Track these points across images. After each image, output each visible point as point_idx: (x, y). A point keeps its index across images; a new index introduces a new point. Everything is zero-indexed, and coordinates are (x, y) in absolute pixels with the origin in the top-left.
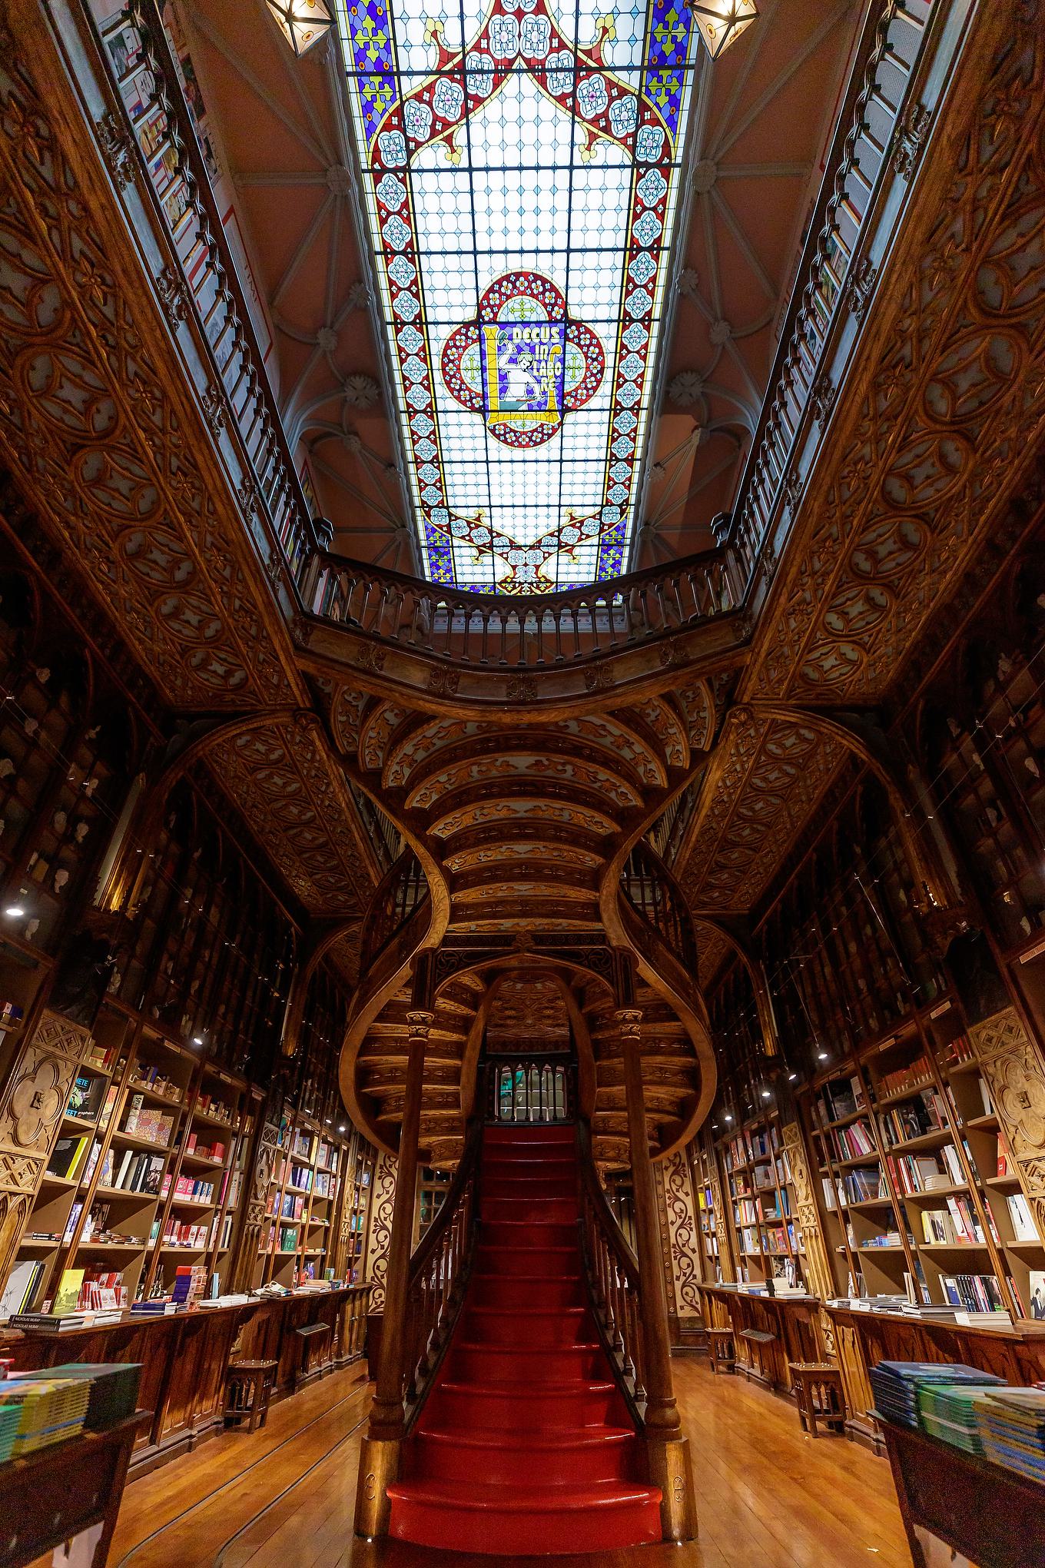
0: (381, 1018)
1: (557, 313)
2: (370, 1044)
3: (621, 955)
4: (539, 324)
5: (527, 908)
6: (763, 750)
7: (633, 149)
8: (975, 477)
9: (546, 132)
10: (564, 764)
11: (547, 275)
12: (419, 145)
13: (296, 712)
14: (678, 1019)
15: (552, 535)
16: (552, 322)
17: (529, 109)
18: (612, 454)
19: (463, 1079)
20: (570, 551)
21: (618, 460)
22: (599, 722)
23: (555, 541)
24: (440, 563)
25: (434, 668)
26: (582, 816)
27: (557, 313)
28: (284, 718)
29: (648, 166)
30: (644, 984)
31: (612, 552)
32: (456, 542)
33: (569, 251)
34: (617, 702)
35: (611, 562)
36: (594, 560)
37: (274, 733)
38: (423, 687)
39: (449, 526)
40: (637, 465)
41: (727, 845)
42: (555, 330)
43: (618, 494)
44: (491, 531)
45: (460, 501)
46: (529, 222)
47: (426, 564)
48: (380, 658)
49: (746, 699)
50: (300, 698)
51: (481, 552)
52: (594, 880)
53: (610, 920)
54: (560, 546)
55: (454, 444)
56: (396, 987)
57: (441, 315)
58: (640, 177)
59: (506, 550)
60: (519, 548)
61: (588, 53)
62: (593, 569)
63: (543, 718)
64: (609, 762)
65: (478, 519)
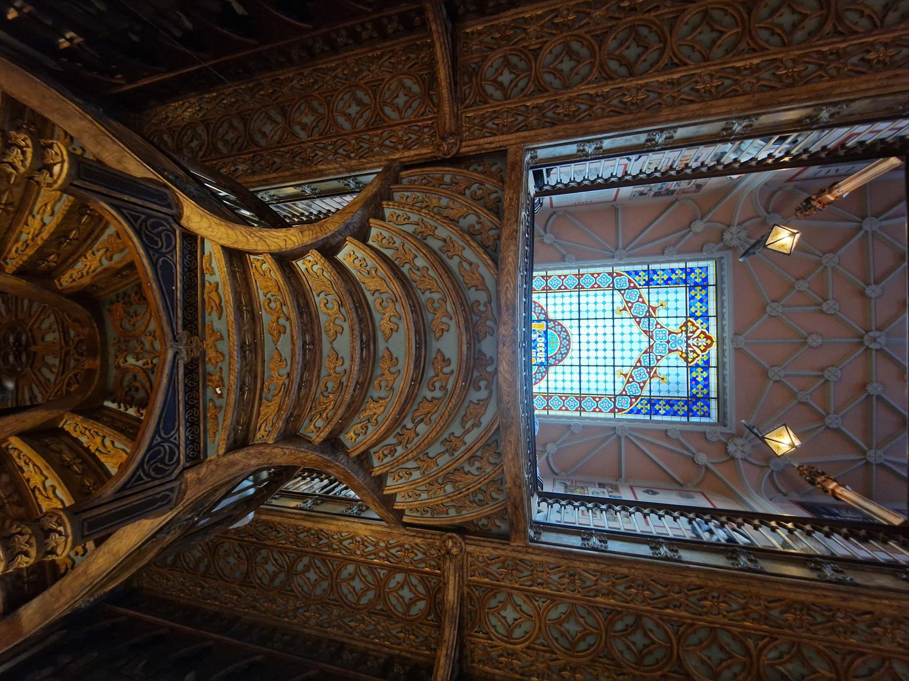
1: (551, 361)
3: (172, 490)
4: (546, 351)
7: (621, 395)
9: (627, 354)
10: (443, 388)
11: (569, 355)
12: (623, 295)
16: (547, 358)
17: (636, 346)
22: (486, 420)
27: (551, 361)
29: (614, 403)
33: (580, 366)
37: (422, 115)
42: (543, 360)
46: (592, 346)
53: (233, 464)
57: (551, 301)
58: (610, 399)
61: (655, 372)
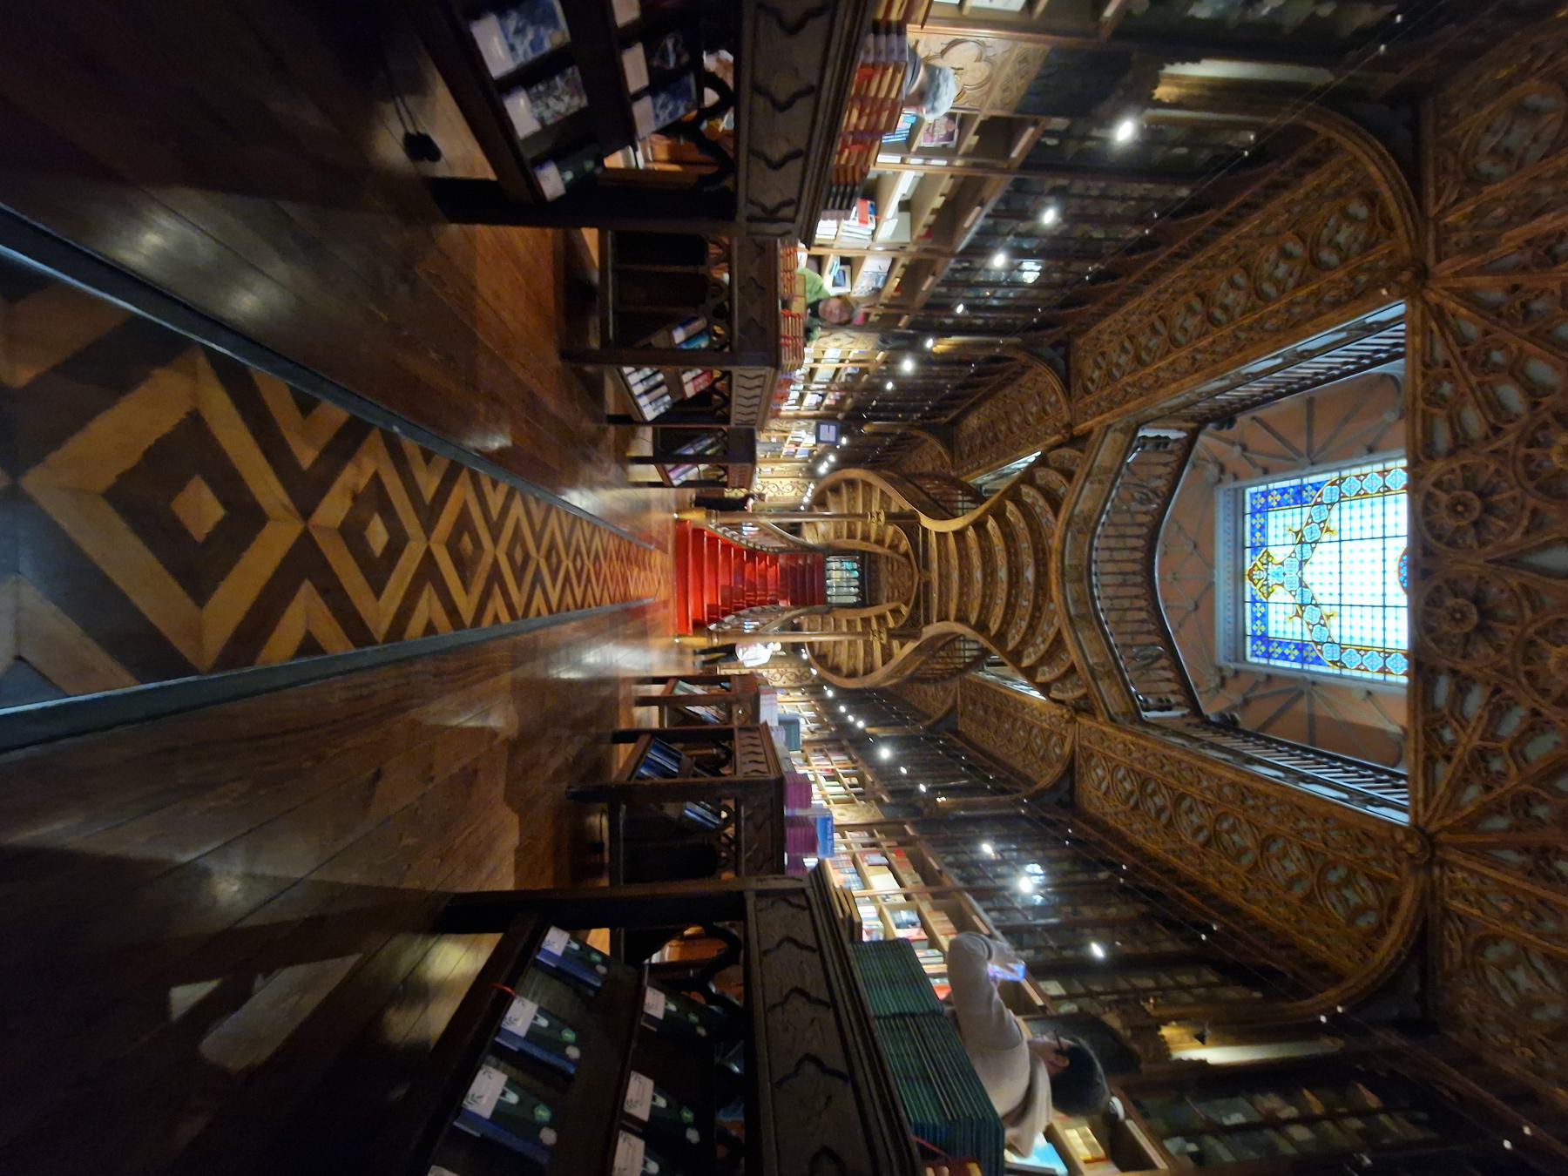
0: (882, 492)
2: (868, 486)
5: (944, 577)
6: (1052, 733)
8: (1191, 849)
13: (1069, 426)
14: (884, 663)
15: (1313, 598)
18: (1390, 654)
19: (850, 541)
20: (1297, 615)
21: (1385, 658)
23: (1307, 601)
24: (1286, 496)
25: (1090, 517)
26: (998, 611)
28: (1067, 418)
30: (902, 646)
31: (1296, 652)
32: (1306, 510)
34: (1067, 636)
35: (1287, 651)
36: (1289, 636)
38: (1077, 511)
39: (1321, 503)
40: (1380, 677)
41: (999, 713)
43: (1352, 659)
44: (1316, 542)
45: (1345, 513)
47: (1285, 484)
48: (1101, 482)
49: (1079, 719)
50: (1081, 427)
51: (1297, 533)
52: (962, 618)
54: (1301, 605)
55: (1356, 512)
56: (900, 503)
59: (1299, 556)
60: (1301, 568)
62: (1280, 635)
63: (1054, 588)
64: (1032, 628)
65: (1328, 530)
